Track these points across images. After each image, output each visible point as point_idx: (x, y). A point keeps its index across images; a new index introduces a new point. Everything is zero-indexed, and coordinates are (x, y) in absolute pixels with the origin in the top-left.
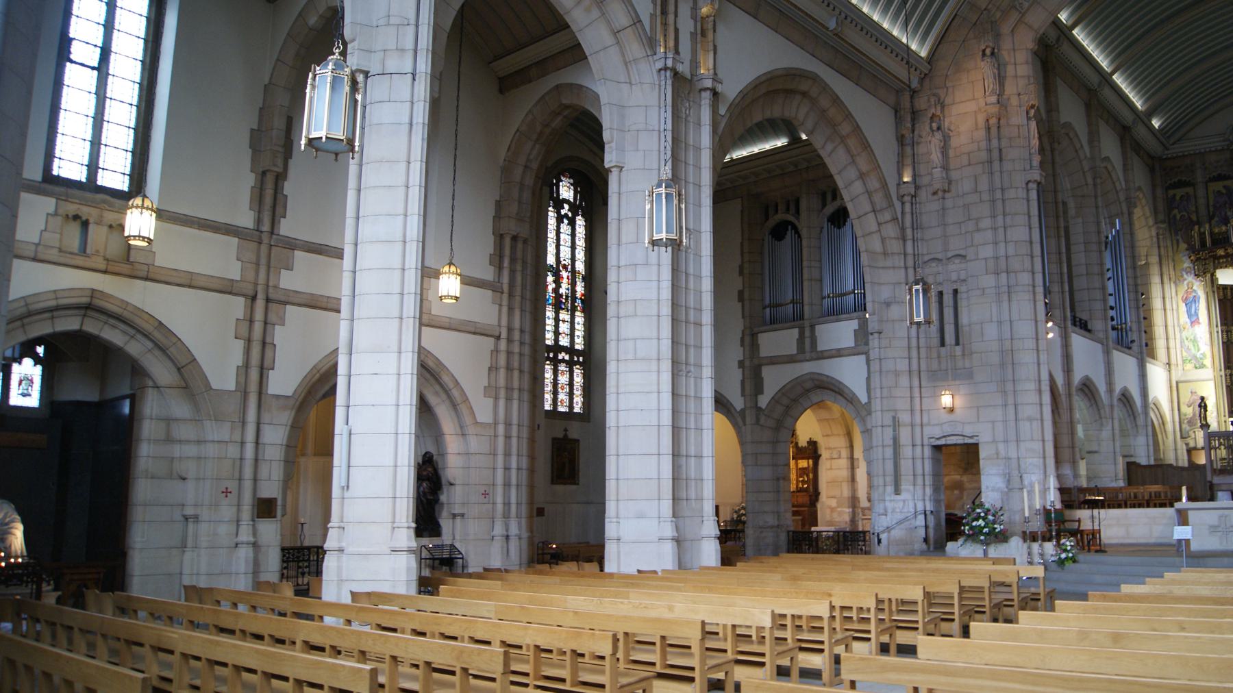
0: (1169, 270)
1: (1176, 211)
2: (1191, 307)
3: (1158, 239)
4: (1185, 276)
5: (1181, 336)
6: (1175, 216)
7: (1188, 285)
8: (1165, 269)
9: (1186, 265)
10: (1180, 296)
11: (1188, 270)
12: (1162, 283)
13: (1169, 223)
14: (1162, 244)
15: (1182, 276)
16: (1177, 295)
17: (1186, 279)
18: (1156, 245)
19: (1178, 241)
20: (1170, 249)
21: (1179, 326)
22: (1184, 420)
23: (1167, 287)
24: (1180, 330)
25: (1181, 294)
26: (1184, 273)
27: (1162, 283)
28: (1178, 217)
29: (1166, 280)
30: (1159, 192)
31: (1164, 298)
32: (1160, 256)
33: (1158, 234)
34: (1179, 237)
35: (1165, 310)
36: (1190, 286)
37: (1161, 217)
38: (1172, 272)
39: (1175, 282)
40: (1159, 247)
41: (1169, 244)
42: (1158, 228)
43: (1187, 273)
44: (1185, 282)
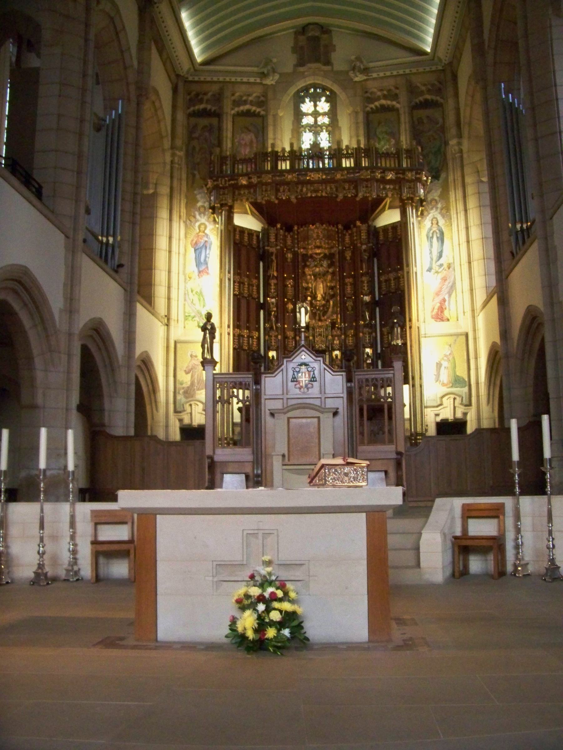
0: (181, 208)
1: (195, 143)
2: (201, 253)
3: (172, 168)
4: (198, 217)
5: (185, 286)
6: (194, 148)
7: (199, 227)
8: (175, 202)
9: (199, 204)
10: (189, 240)
11: (202, 210)
12: (171, 220)
13: (187, 151)
14: (176, 174)
15: (195, 217)
16: (186, 237)
17: (197, 221)
18: (169, 175)
19: (194, 175)
20: (184, 183)
21: (184, 274)
22: (180, 389)
23: (175, 225)
24: (185, 279)
25: (192, 236)
26: (197, 213)
27: (171, 220)
28: (197, 149)
29: (175, 217)
30: (180, 116)
31: (170, 238)
32: (172, 189)
33: (172, 162)
34: (196, 172)
35: (170, 252)
36: (202, 228)
37: (179, 142)
38: (183, 210)
39: (185, 222)
40: (172, 177)
41: (184, 176)
42: (173, 155)
43: (200, 214)
44: (197, 224)
